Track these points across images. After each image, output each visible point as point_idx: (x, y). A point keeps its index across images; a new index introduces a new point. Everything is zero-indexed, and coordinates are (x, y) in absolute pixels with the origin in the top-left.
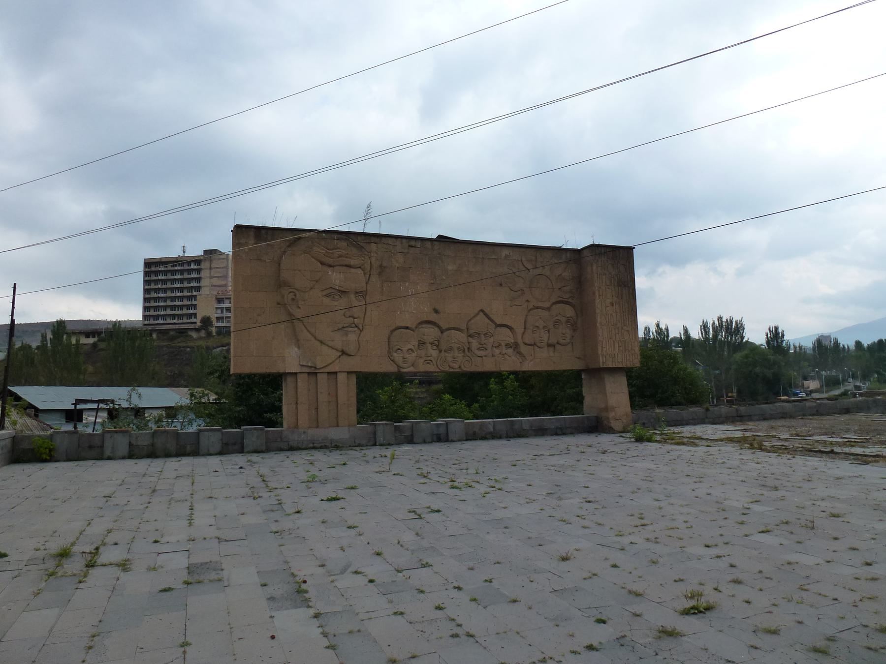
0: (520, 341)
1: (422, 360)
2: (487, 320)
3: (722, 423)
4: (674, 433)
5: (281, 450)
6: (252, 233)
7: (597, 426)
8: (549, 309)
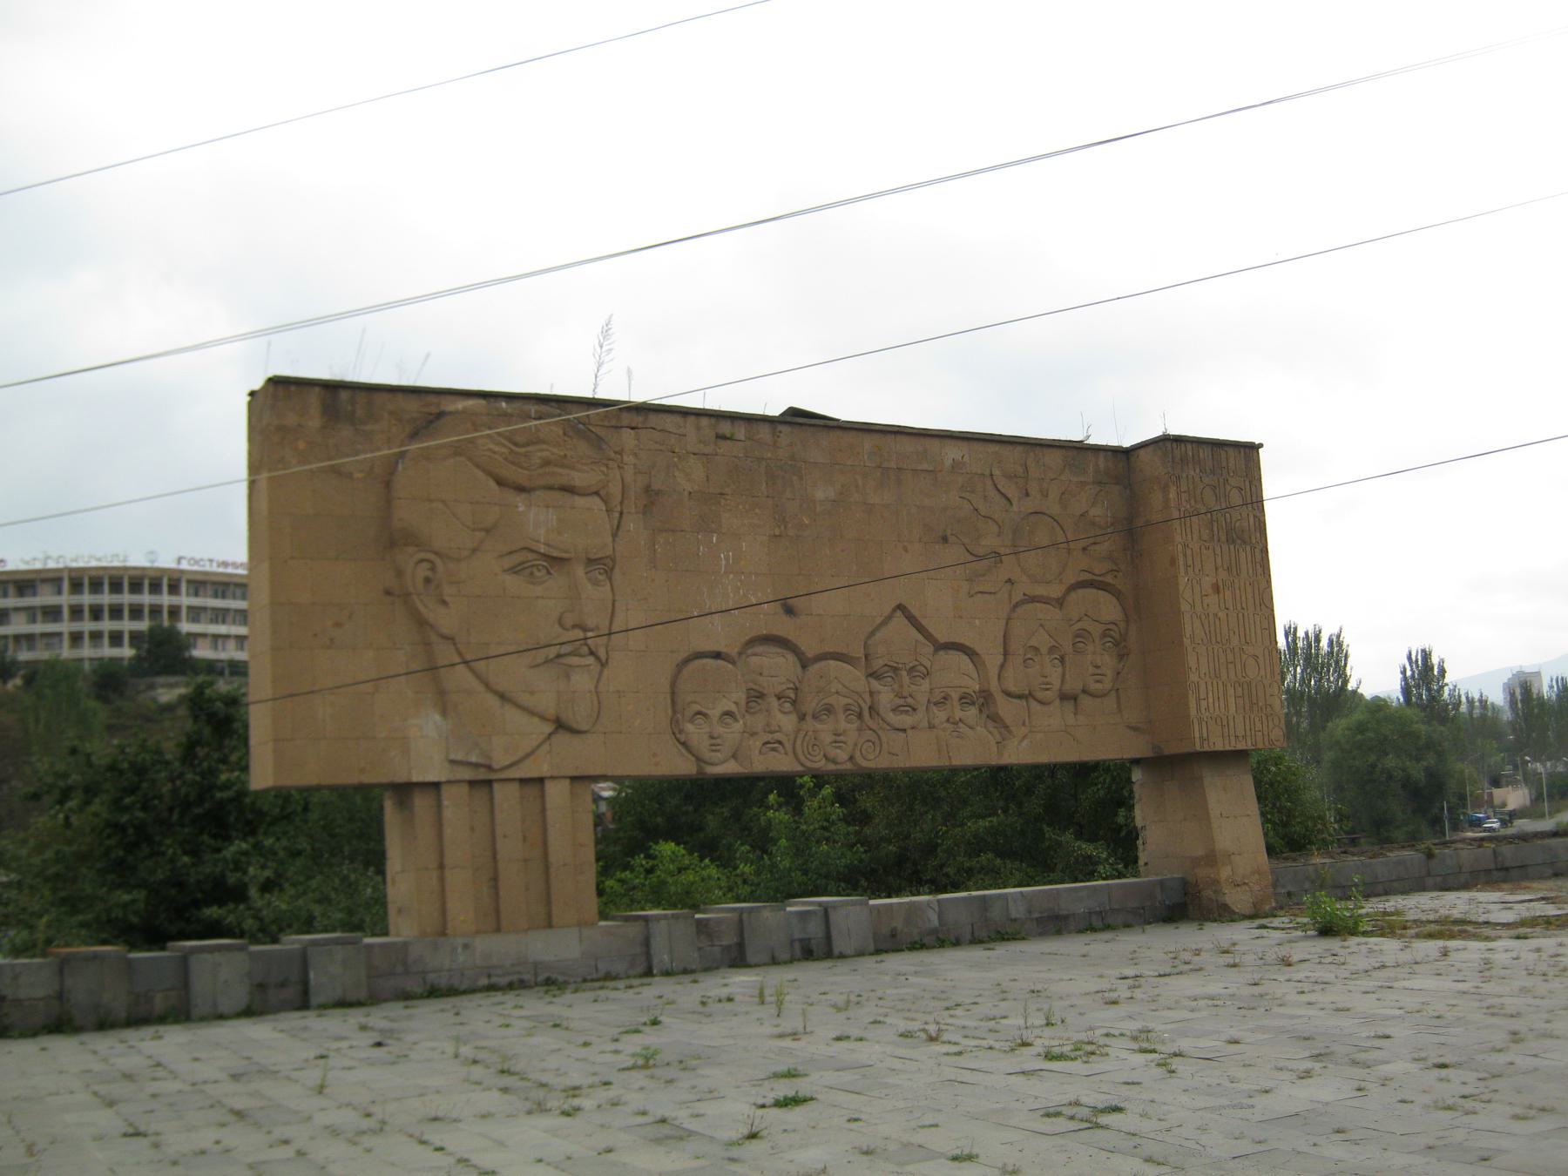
0: (994, 686)
1: (759, 744)
2: (913, 632)
3: (1465, 887)
4: (1385, 913)
5: (406, 996)
6: (314, 397)
7: (1185, 904)
8: (1060, 602)
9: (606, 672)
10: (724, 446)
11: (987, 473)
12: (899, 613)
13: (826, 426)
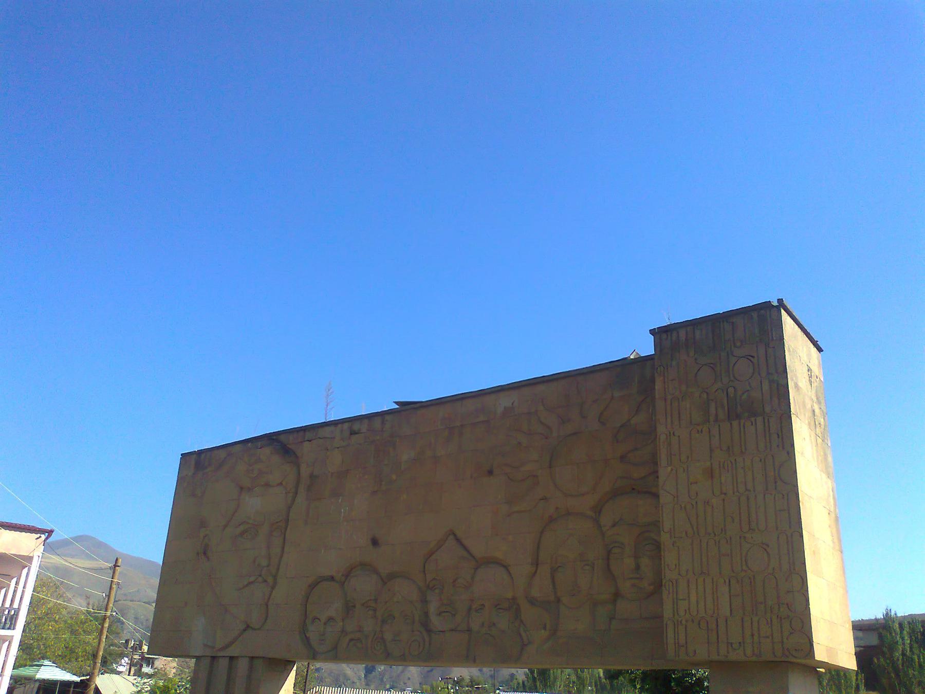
10: (354, 437)
12: (452, 537)
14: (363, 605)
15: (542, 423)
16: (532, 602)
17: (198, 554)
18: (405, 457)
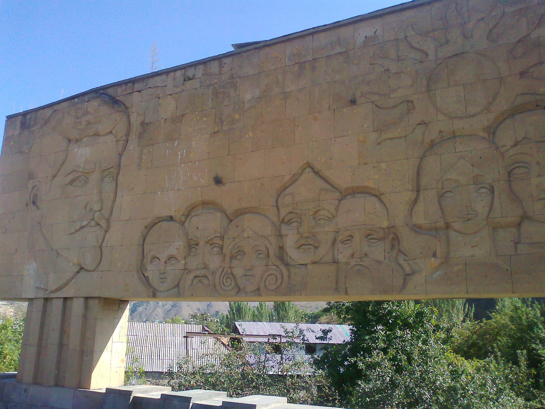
1: (191, 276)
9: (107, 234)
10: (189, 84)
11: (401, 36)
12: (308, 170)
13: (256, 48)
14: (207, 243)
15: (413, 47)
16: (417, 229)
17: (27, 205)
18: (248, 97)
